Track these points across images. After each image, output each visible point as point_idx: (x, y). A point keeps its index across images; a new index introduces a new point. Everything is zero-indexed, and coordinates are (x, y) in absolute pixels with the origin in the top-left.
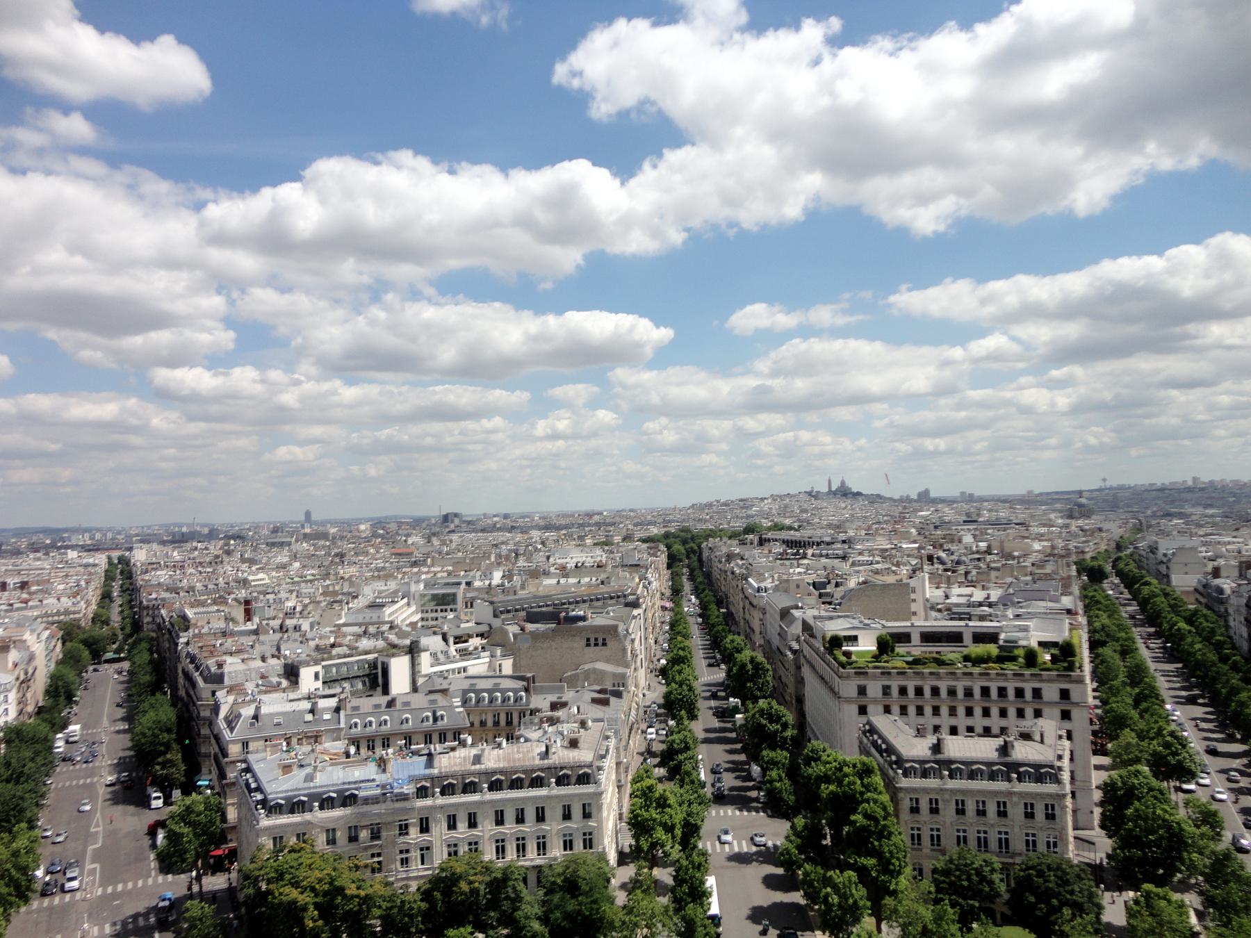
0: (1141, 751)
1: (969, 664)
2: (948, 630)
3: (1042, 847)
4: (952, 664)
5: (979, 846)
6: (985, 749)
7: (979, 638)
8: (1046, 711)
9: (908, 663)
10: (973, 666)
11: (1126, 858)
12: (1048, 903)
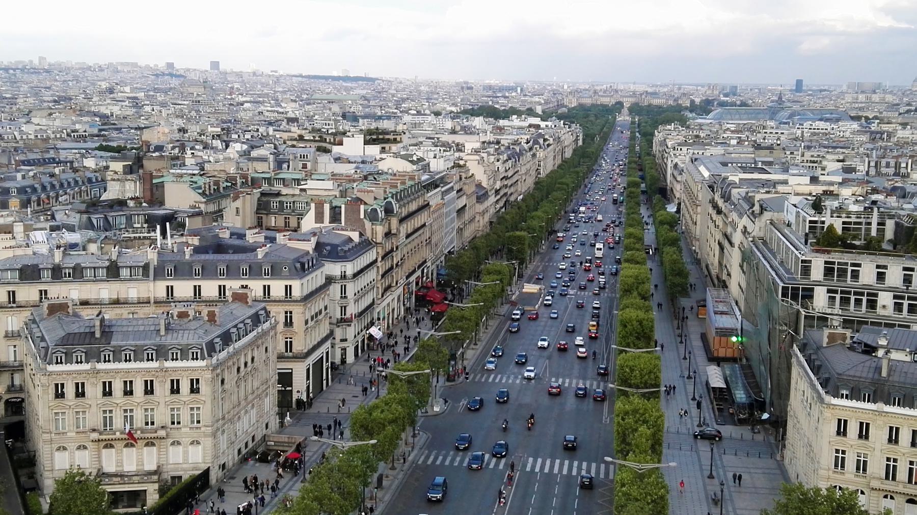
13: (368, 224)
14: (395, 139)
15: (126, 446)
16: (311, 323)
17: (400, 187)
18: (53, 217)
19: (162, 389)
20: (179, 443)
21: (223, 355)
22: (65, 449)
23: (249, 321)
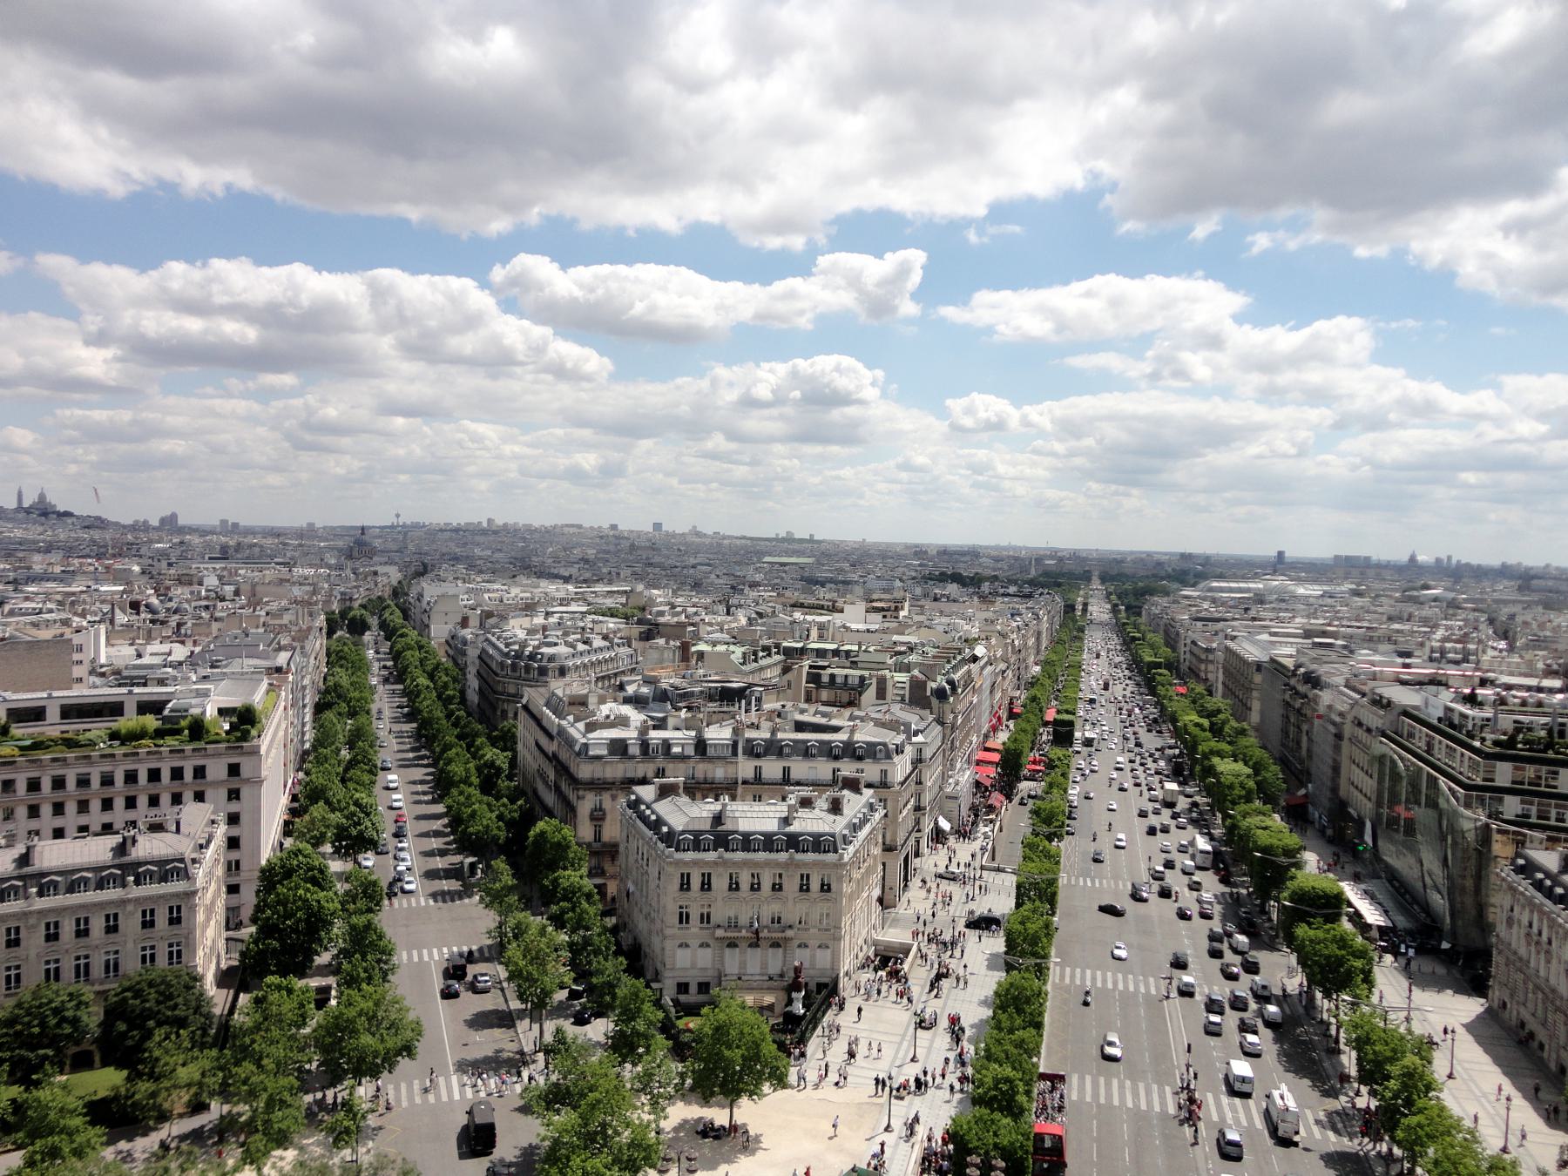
0: (328, 827)
1: (117, 743)
2: (102, 700)
3: (162, 961)
4: (92, 744)
5: (78, 975)
6: (98, 850)
7: (144, 708)
8: (209, 794)
9: (22, 748)
10: (123, 744)
11: (260, 952)
12: (142, 1027)
13: (935, 701)
14: (896, 607)
15: (750, 946)
16: (905, 812)
17: (954, 662)
18: (621, 687)
19: (791, 885)
20: (806, 946)
21: (851, 849)
22: (687, 946)
23: (865, 810)
